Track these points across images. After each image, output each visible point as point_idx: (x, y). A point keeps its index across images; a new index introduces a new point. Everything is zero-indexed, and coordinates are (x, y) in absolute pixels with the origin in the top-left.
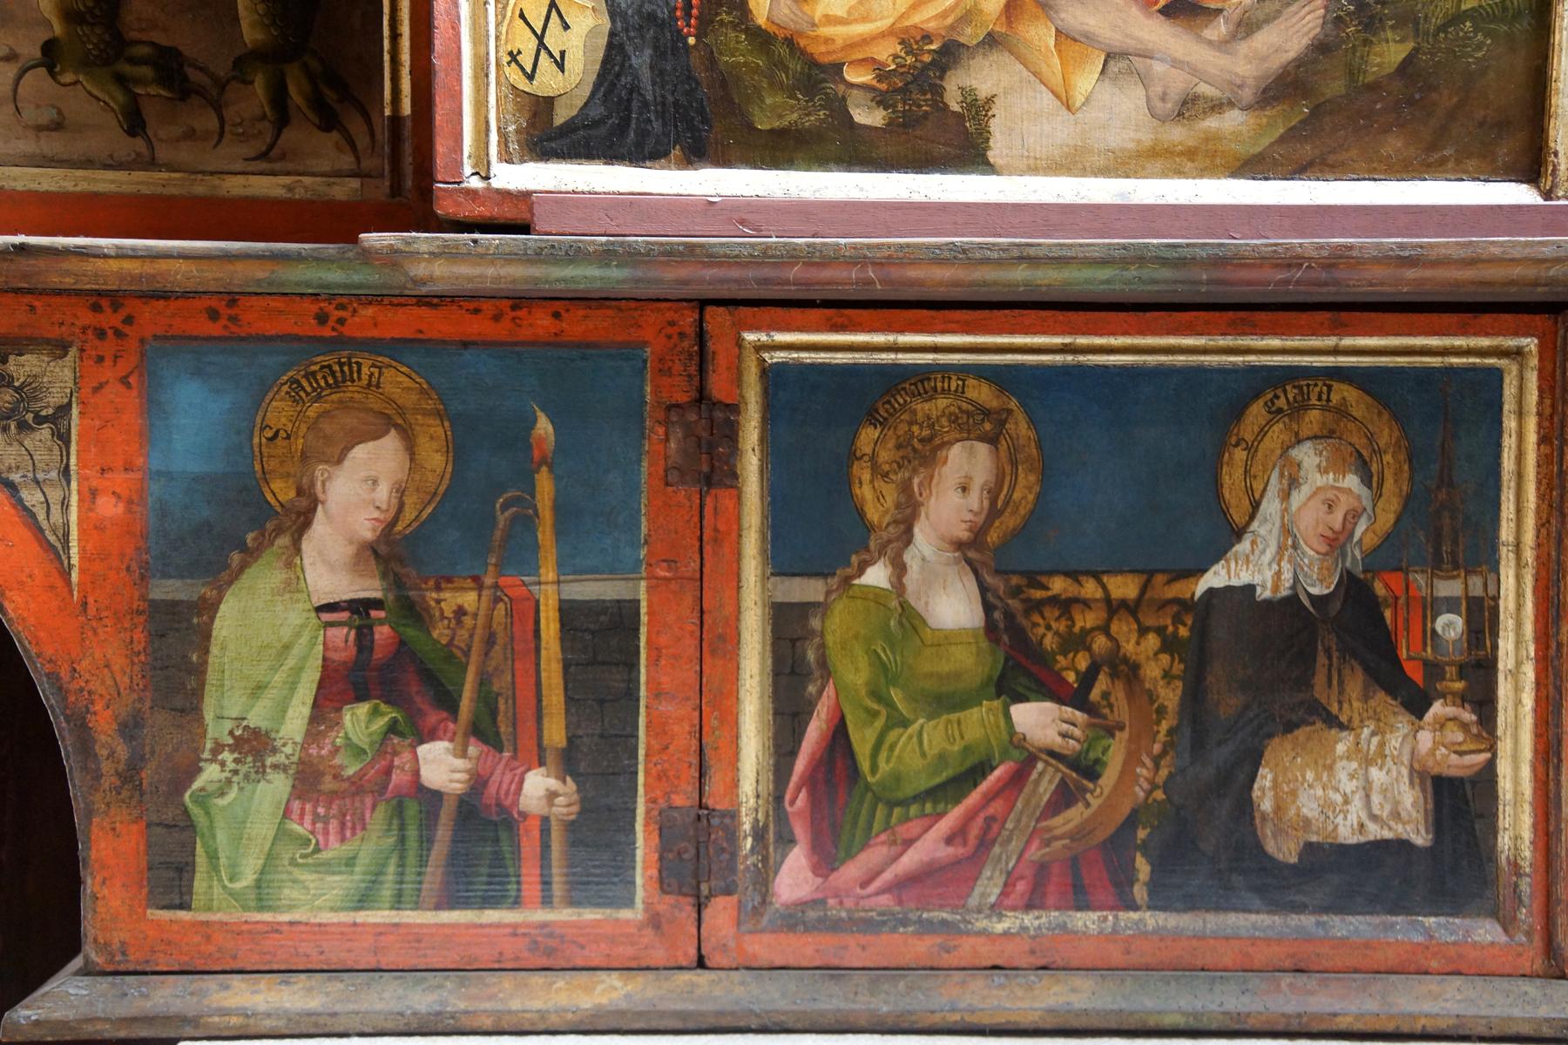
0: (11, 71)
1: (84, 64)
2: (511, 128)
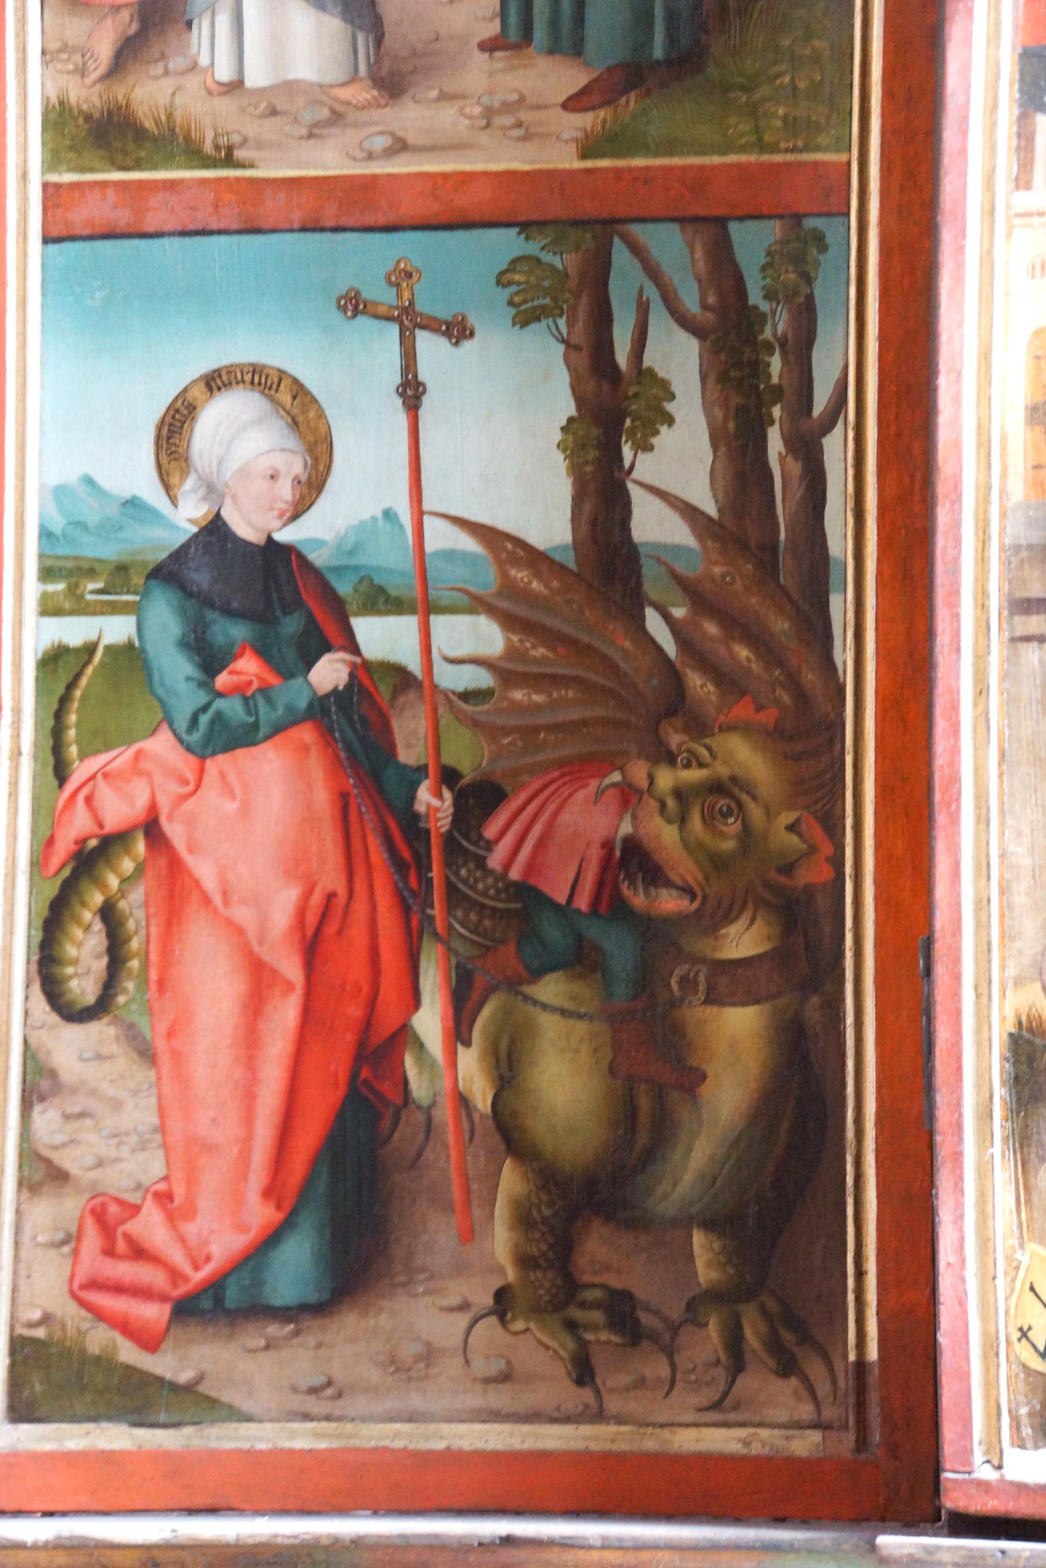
0: (462, 1320)
1: (536, 1310)
2: (1024, 1411)
